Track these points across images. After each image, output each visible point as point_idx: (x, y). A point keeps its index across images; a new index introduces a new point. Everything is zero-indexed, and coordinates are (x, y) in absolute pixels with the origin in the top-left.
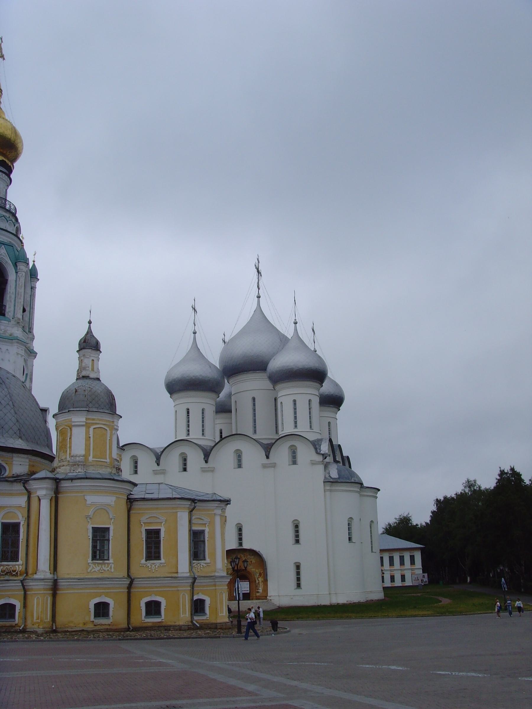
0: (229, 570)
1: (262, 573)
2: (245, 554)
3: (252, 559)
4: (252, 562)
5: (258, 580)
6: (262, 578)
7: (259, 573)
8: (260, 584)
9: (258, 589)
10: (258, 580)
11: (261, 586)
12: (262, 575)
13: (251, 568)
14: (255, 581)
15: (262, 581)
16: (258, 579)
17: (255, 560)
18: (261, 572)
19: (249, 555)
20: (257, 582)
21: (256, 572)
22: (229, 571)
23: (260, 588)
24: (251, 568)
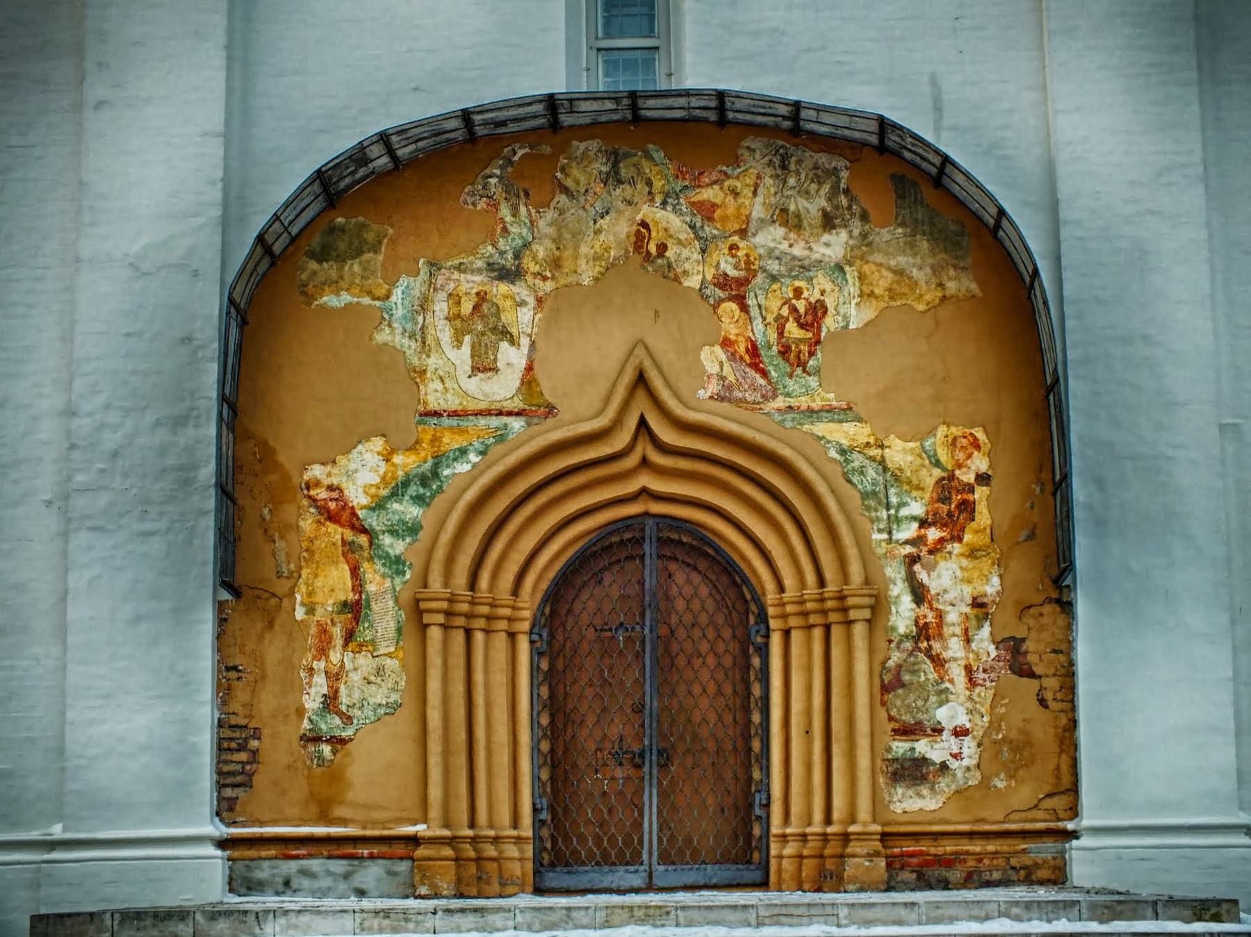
0: (451, 442)
1: (983, 479)
2: (707, 211)
3: (822, 281)
4: (830, 323)
5: (919, 594)
6: (972, 553)
7: (930, 477)
8: (954, 649)
9: (908, 731)
10: (919, 594)
11: (957, 673)
12: (983, 517)
13: (812, 414)
14: (879, 606)
15: (977, 603)
16: (922, 575)
17: (867, 295)
18: (968, 477)
19: (789, 220)
20: (903, 614)
21: (882, 462)
22: (463, 452)
23: (942, 715)
24: (812, 414)
